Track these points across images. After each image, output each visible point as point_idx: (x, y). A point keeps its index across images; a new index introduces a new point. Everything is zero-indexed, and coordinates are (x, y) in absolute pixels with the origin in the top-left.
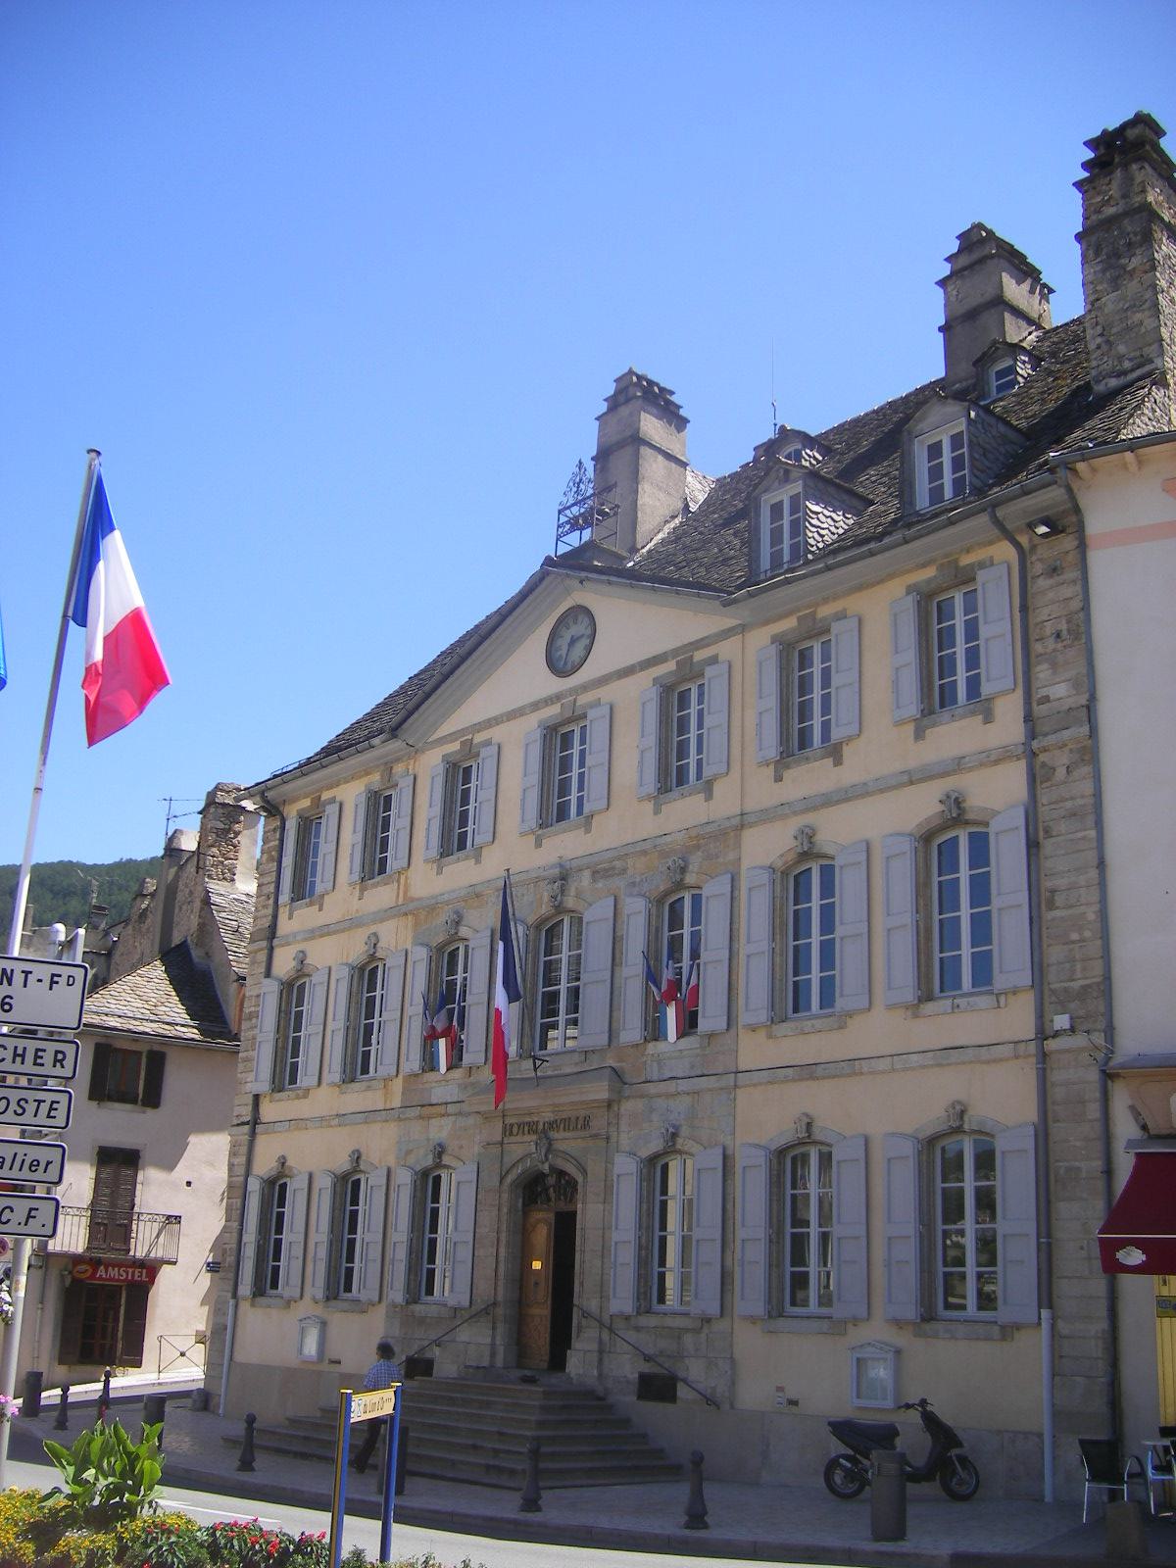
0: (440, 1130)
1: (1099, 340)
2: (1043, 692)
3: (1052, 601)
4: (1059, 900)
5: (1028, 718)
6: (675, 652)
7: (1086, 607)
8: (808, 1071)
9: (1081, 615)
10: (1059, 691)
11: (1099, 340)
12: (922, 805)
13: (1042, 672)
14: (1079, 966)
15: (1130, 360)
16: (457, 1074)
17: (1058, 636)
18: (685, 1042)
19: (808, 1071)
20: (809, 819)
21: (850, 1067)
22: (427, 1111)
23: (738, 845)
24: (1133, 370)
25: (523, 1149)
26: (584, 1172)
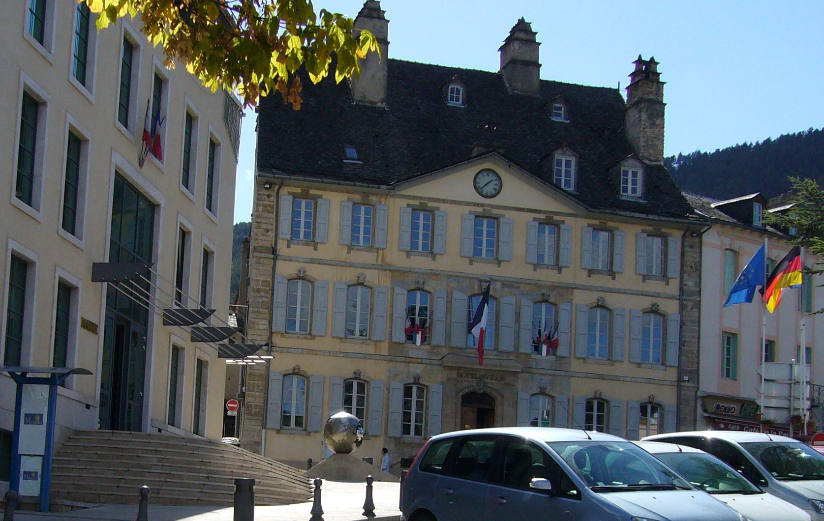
0: (417, 369)
1: (644, 144)
2: (685, 282)
3: (691, 255)
4: (686, 344)
5: (681, 289)
6: (546, 212)
7: (700, 262)
8: (601, 377)
9: (699, 264)
10: (690, 284)
11: (644, 144)
12: (646, 303)
13: (686, 276)
14: (690, 364)
15: (654, 157)
16: (427, 347)
17: (691, 267)
18: (549, 357)
19: (601, 377)
20: (602, 294)
21: (616, 378)
22: (408, 360)
23: (572, 294)
24: (654, 161)
25: (469, 384)
26: (502, 396)
